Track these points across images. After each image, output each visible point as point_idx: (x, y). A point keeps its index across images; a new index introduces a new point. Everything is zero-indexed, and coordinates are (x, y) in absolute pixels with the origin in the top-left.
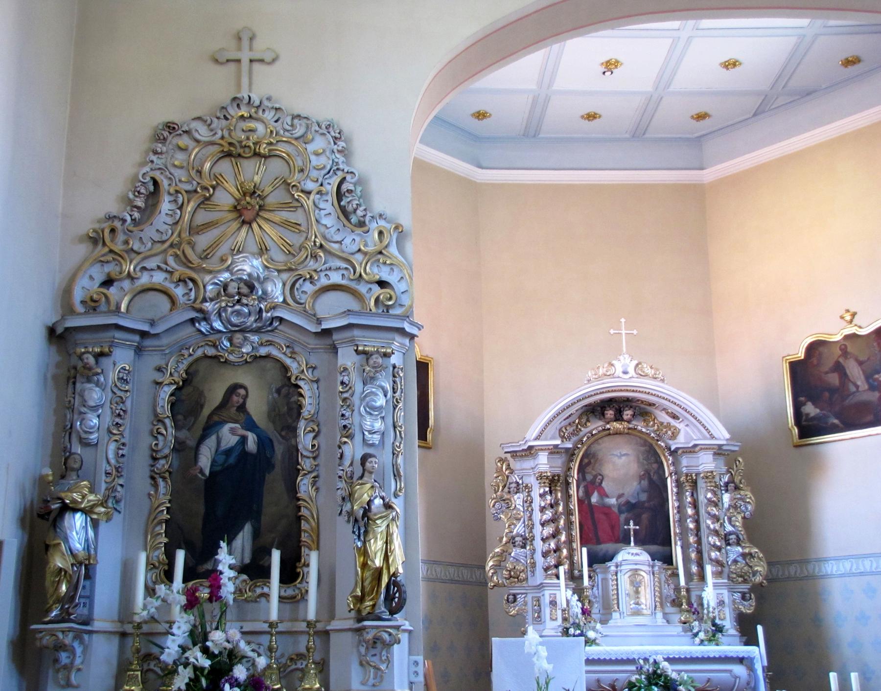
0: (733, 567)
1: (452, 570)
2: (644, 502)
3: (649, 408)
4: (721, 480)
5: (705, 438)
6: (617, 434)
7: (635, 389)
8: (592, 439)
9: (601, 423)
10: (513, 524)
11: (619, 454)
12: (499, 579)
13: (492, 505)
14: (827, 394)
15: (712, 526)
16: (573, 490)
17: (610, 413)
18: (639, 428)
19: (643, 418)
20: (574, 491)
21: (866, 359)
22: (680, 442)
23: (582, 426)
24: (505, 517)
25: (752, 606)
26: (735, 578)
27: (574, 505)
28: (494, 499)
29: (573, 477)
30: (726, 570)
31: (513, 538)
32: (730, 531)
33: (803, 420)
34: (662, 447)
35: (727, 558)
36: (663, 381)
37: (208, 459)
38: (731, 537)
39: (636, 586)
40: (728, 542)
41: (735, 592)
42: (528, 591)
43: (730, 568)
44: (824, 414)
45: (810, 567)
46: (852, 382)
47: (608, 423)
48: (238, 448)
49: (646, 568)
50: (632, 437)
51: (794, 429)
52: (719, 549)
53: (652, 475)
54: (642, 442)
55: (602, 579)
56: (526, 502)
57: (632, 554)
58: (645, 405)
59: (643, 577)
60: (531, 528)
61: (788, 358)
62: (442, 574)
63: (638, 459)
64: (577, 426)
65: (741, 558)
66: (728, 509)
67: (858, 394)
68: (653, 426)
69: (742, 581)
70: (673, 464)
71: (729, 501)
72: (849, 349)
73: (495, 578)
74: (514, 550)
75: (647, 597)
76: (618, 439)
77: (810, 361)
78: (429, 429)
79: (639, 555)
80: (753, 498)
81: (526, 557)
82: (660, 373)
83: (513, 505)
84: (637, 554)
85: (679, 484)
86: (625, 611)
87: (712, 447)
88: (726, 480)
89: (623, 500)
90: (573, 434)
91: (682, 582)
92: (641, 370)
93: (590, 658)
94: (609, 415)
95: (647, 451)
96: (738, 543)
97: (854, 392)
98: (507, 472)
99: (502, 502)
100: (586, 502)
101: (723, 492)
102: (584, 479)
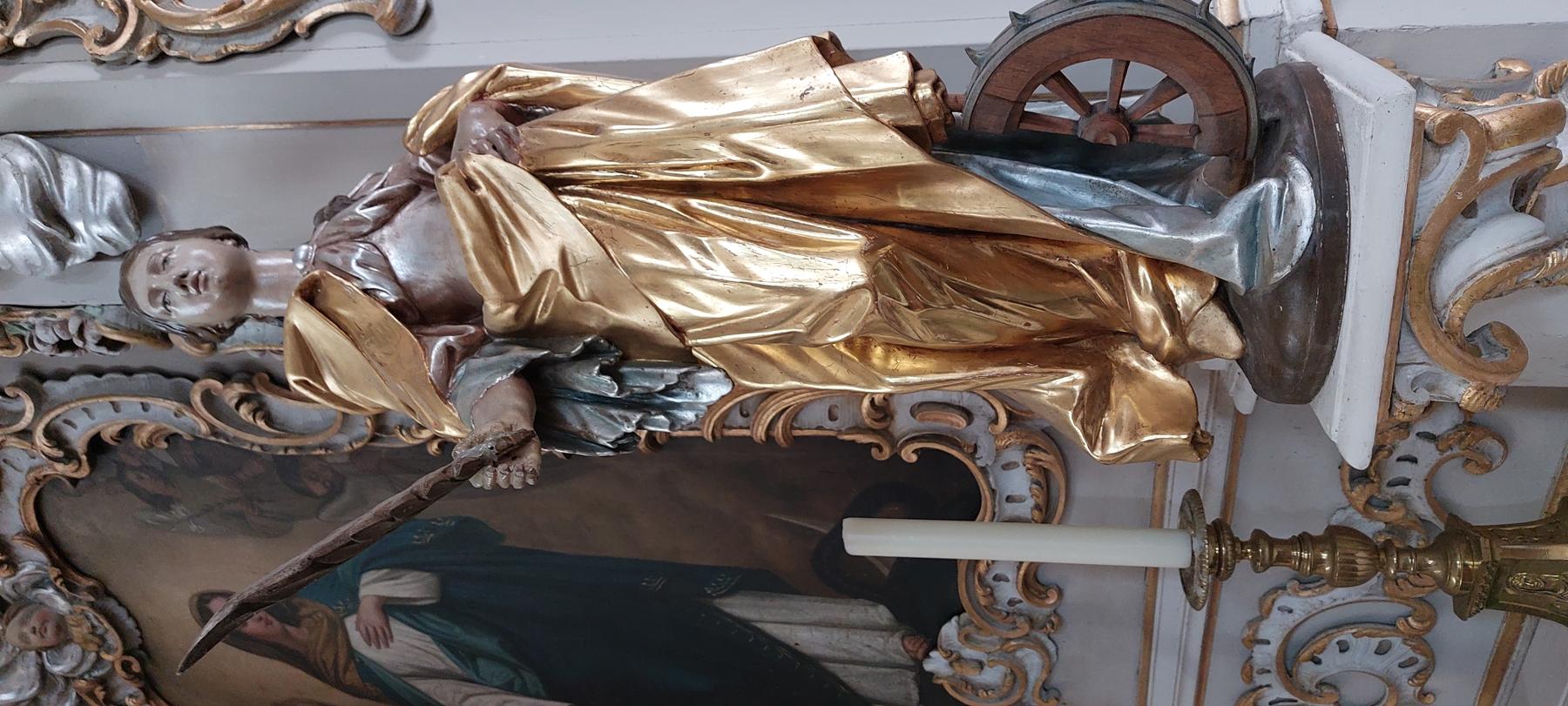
37: (505, 702)
48: (432, 625)
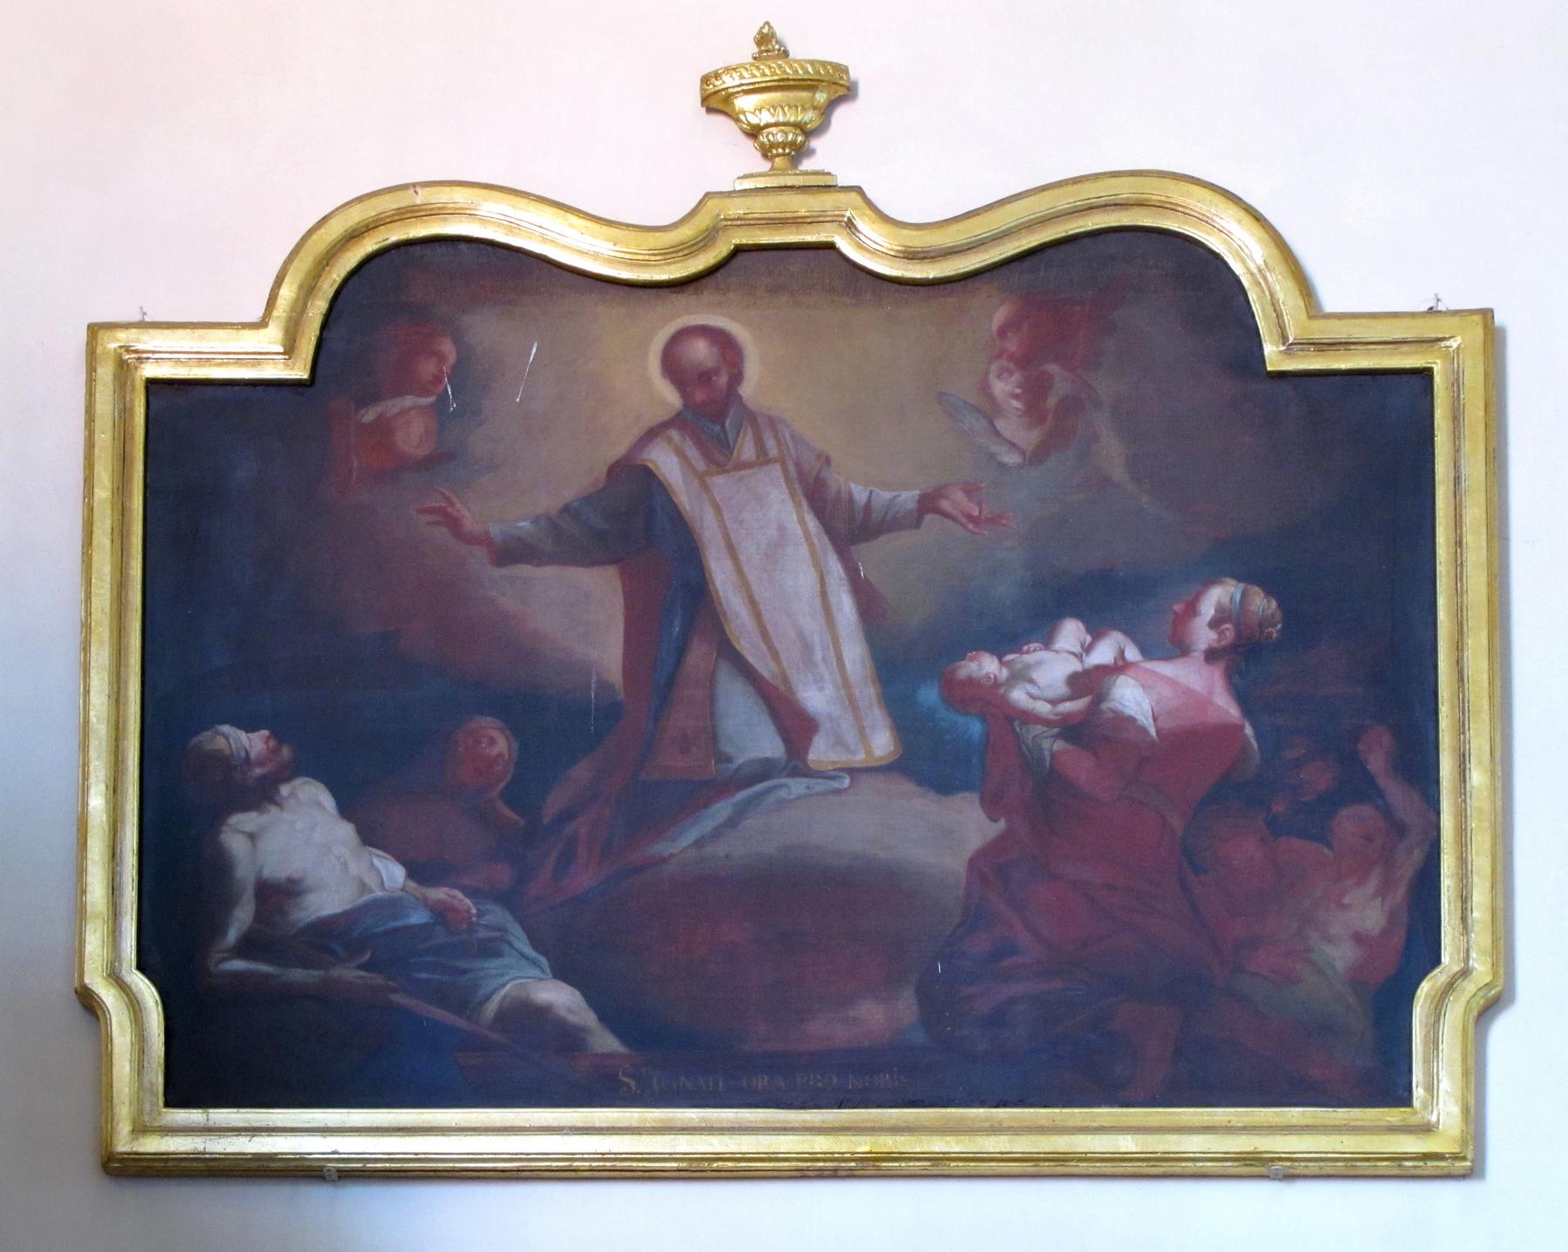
14: (499, 744)
21: (908, 498)
33: (232, 935)
44: (441, 914)
67: (797, 786)
72: (753, 386)
77: (369, 415)
97: (765, 771)
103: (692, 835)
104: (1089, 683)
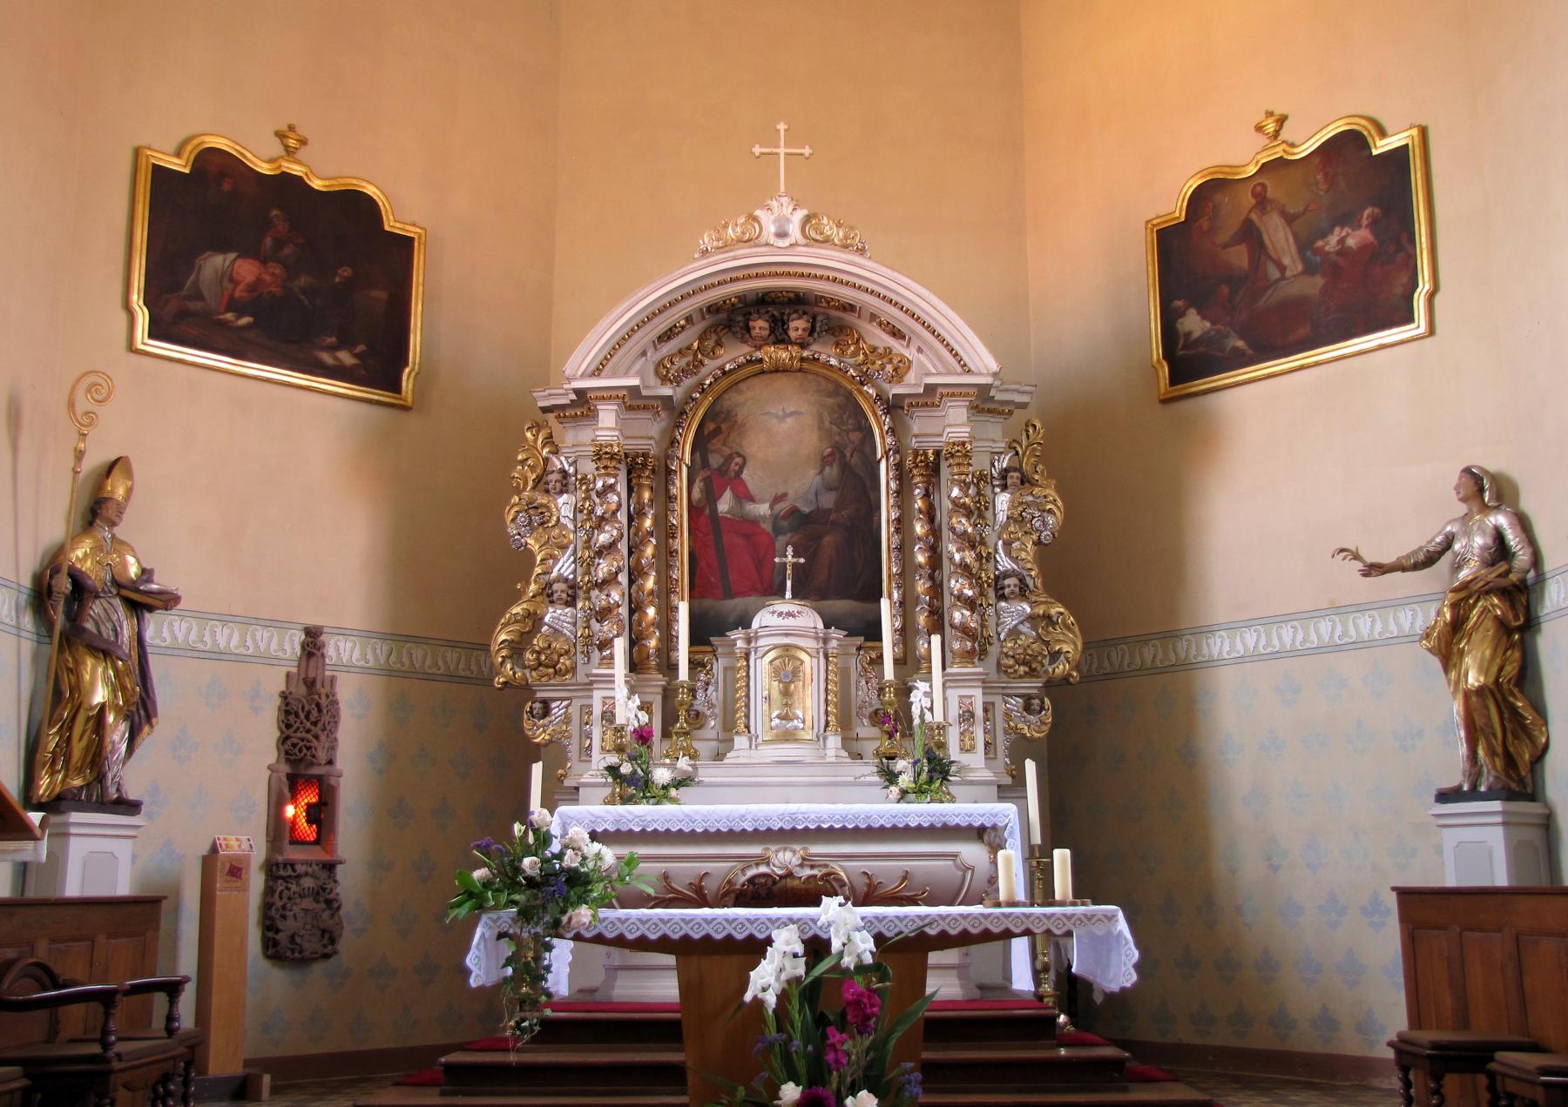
0: (1009, 645)
1: (452, 656)
2: (830, 510)
3: (849, 318)
4: (993, 465)
5: (950, 373)
6: (777, 371)
7: (806, 271)
8: (725, 383)
9: (745, 349)
10: (552, 556)
11: (780, 413)
12: (517, 669)
13: (511, 517)
14: (1225, 289)
15: (957, 557)
16: (680, 485)
17: (760, 326)
18: (823, 357)
19: (833, 339)
20: (681, 490)
21: (1301, 209)
22: (911, 384)
23: (707, 356)
24: (537, 540)
25: (1046, 724)
26: (1011, 667)
27: (680, 516)
28: (514, 505)
29: (681, 460)
30: (994, 650)
31: (549, 584)
32: (1007, 571)
33: (1180, 347)
34: (871, 396)
35: (997, 625)
36: (861, 251)
38: (1007, 582)
39: (787, 676)
40: (1001, 592)
41: (1010, 696)
42: (574, 694)
43: (1002, 647)
44: (1218, 331)
45: (1182, 646)
46: (1273, 260)
47: (759, 348)
49: (810, 644)
50: (811, 377)
51: (1162, 366)
52: (971, 604)
53: (848, 454)
54: (831, 387)
55: (725, 669)
56: (581, 511)
57: (780, 614)
58: (837, 308)
59: (802, 662)
60: (588, 564)
61: (1155, 222)
62: (428, 663)
63: (821, 421)
64: (695, 355)
65: (1028, 625)
66: (1005, 526)
67: (1284, 283)
68: (855, 354)
69: (1025, 673)
70: (892, 431)
71: (1009, 509)
72: (1270, 194)
73: (509, 666)
74: (551, 610)
75: (810, 703)
76: (781, 381)
77: (1197, 224)
78: (407, 370)
79: (794, 616)
80: (1060, 503)
81: (575, 624)
82: (856, 234)
83: (555, 518)
84: (790, 614)
85: (901, 473)
86: (759, 732)
87: (964, 390)
88: (1005, 466)
89: (783, 507)
90: (685, 372)
91: (889, 672)
92: (816, 230)
93: (599, 830)
94: (757, 330)
95: (839, 406)
96: (1023, 592)
97: (1277, 281)
98: (545, 451)
99: (531, 512)
100: (707, 511)
101: (997, 490)
102: (705, 464)
103: (1264, 299)
104: (1342, 241)
